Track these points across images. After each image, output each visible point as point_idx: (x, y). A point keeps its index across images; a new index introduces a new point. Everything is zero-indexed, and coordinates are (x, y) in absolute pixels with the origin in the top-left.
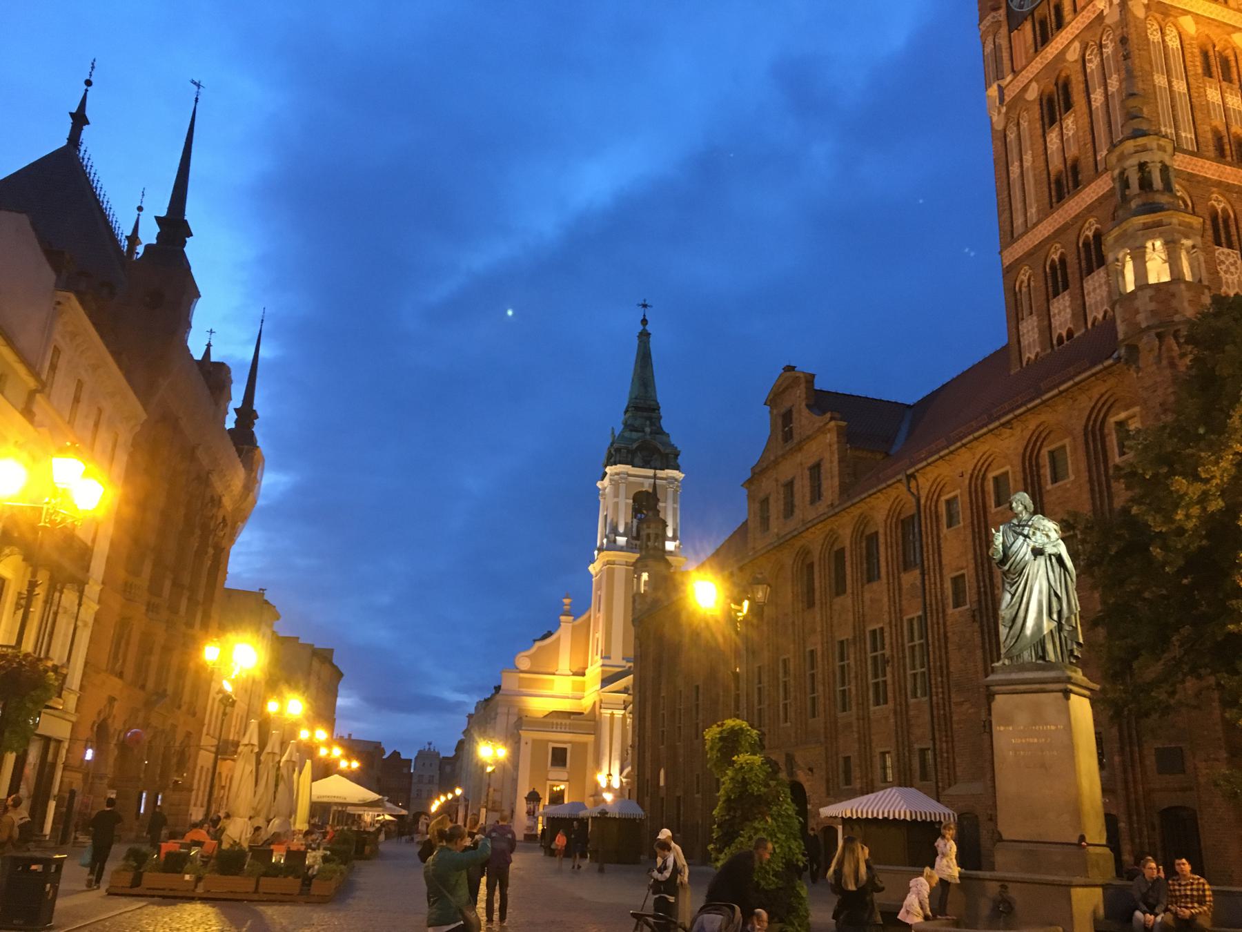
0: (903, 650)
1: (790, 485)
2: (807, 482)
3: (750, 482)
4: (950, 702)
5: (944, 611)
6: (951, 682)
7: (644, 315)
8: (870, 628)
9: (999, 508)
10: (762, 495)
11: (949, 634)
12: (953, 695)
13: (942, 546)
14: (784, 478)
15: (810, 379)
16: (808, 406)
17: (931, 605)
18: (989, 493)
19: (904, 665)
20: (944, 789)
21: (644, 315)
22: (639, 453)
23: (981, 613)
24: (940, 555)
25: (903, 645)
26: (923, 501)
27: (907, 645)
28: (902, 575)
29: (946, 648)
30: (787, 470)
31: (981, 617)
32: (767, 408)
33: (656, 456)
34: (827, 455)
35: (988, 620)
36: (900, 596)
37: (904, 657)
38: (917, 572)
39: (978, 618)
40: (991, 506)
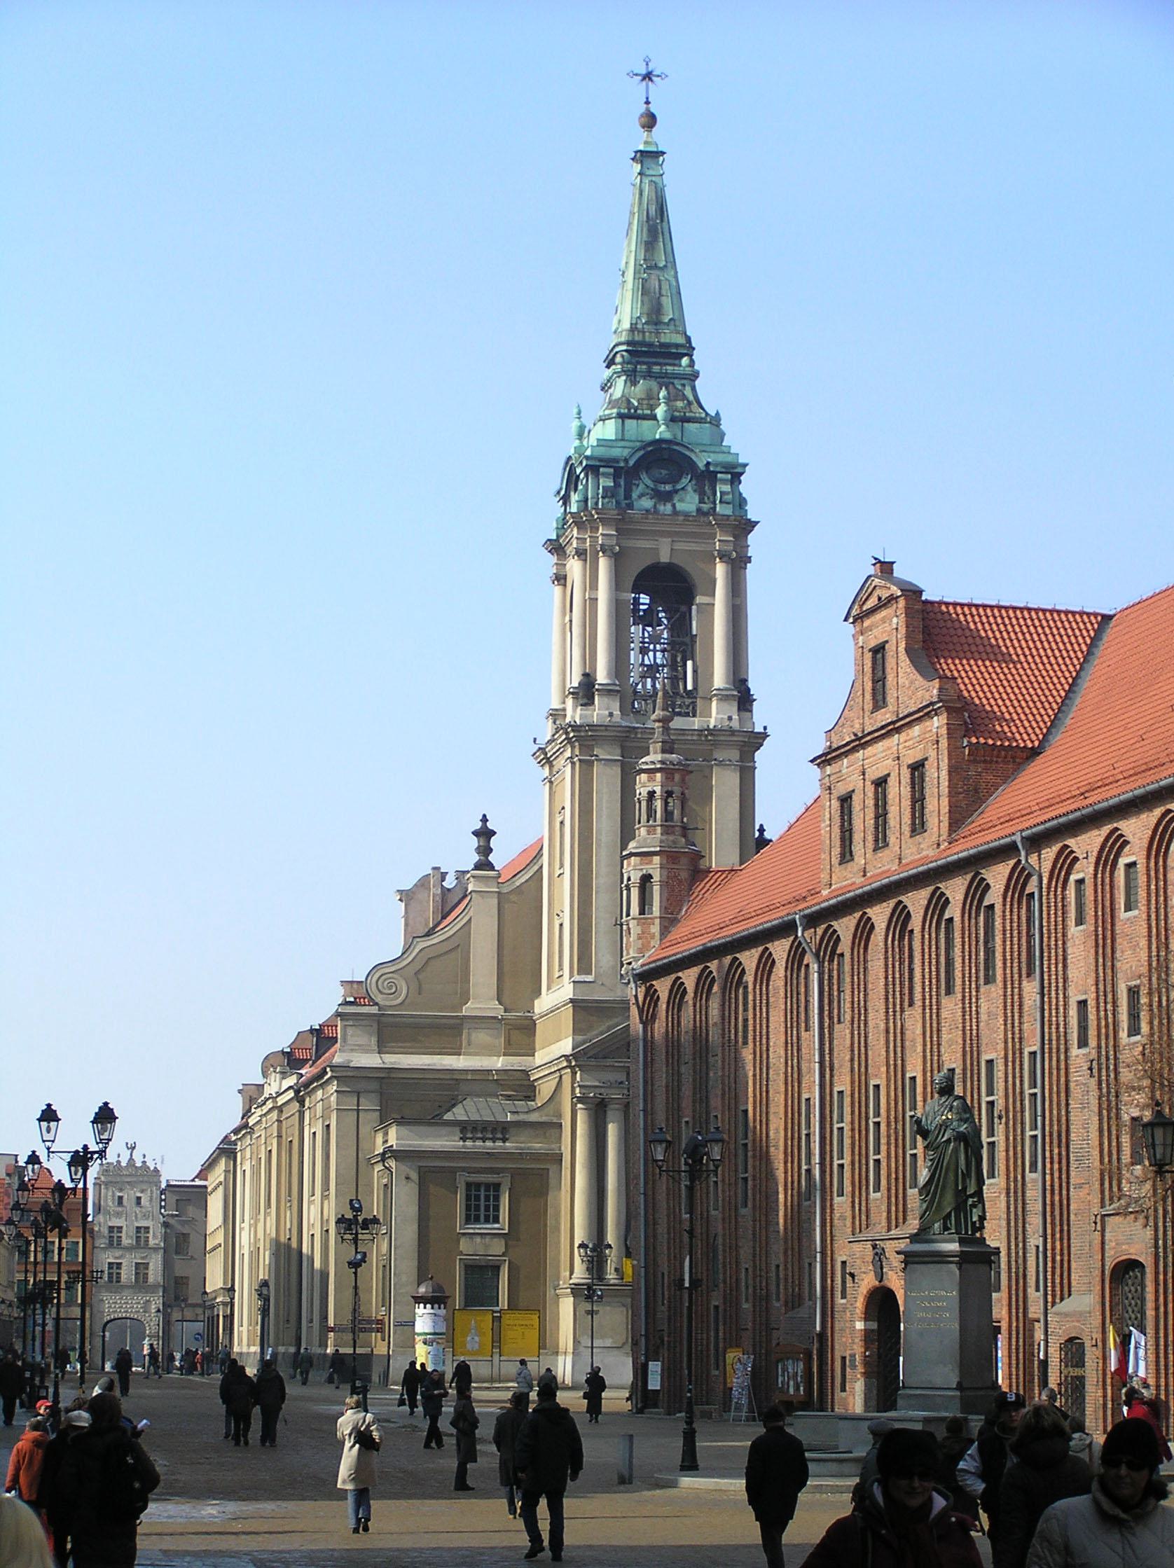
0: (1022, 1101)
1: (881, 783)
2: (906, 791)
3: (823, 760)
4: (1068, 1183)
5: (1067, 1050)
6: (1072, 1158)
7: (647, 103)
8: (985, 1057)
9: (1130, 914)
10: (841, 789)
11: (1072, 1085)
12: (1072, 1174)
13: (1069, 951)
14: (874, 773)
15: (912, 593)
16: (908, 650)
17: (1050, 1040)
18: (1119, 887)
19: (1023, 1123)
20: (1054, 1304)
21: (647, 103)
22: (644, 476)
23: (1099, 1064)
24: (1065, 966)
25: (1022, 1093)
26: (1045, 881)
27: (1027, 1092)
28: (1025, 983)
29: (1067, 1105)
30: (879, 759)
31: (1100, 1070)
32: (849, 628)
33: (685, 481)
34: (932, 754)
35: (1108, 1076)
36: (1020, 1017)
37: (1022, 1111)
38: (1036, 983)
39: (1095, 1071)
40: (1120, 909)
